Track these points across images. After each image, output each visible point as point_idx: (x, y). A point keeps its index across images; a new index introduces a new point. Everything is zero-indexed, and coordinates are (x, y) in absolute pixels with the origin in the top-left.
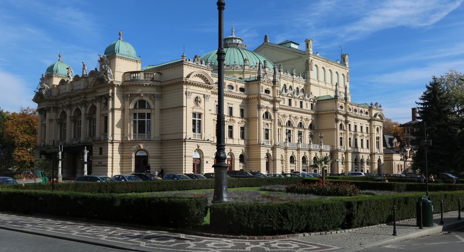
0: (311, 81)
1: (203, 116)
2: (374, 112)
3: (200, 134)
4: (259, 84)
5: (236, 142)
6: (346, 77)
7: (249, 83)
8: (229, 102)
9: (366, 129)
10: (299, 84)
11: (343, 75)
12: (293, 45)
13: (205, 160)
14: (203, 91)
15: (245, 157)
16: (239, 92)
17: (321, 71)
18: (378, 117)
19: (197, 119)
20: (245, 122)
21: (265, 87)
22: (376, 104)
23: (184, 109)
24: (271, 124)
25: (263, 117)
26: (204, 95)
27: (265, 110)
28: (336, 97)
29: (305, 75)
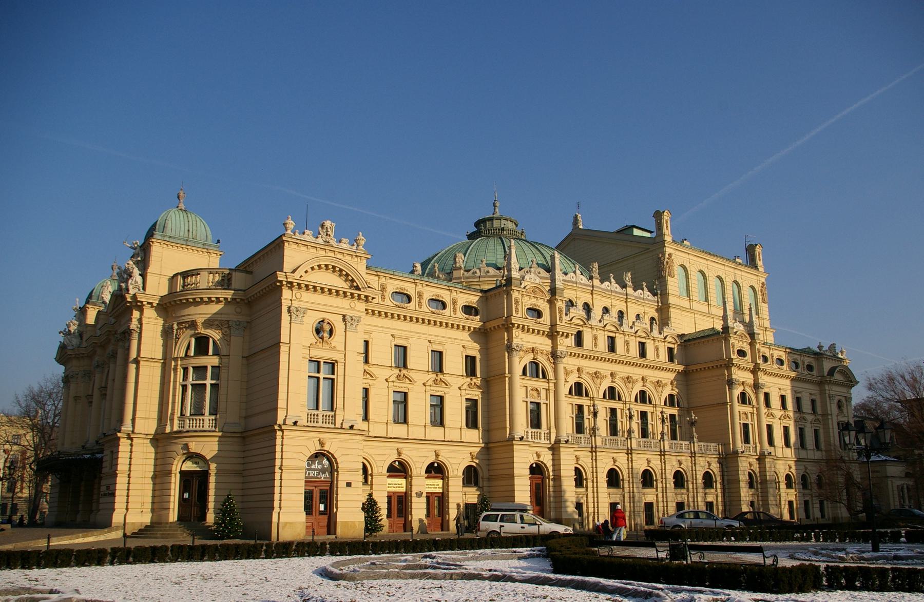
0: (672, 300)
1: (340, 369)
2: (827, 365)
3: (332, 413)
4: (509, 295)
5: (452, 435)
6: (759, 293)
7: (488, 294)
8: (432, 338)
9: (809, 403)
10: (642, 304)
11: (752, 287)
12: (636, 232)
13: (343, 478)
14: (343, 305)
15: (480, 474)
16: (460, 314)
17: (695, 278)
18: (837, 377)
19: (321, 375)
20: (478, 387)
21: (528, 302)
22: (832, 347)
23: (283, 349)
24: (547, 390)
25: (524, 373)
26: (344, 316)
27: (529, 358)
28: (726, 329)
29: (658, 288)
